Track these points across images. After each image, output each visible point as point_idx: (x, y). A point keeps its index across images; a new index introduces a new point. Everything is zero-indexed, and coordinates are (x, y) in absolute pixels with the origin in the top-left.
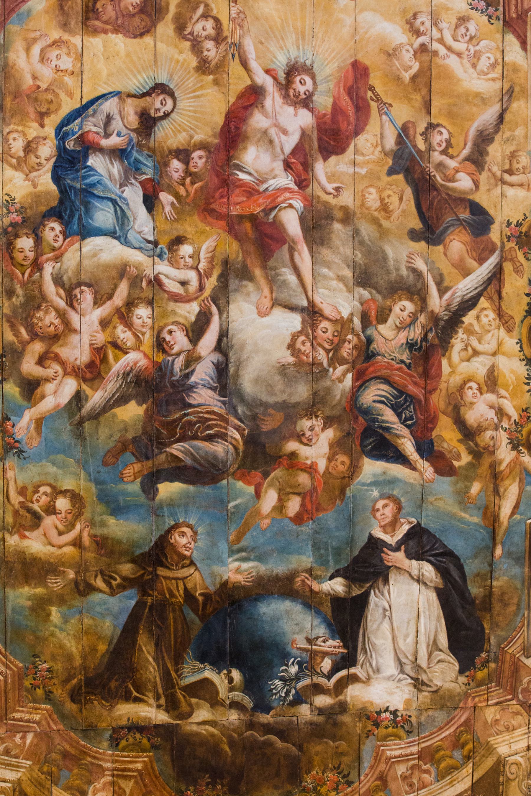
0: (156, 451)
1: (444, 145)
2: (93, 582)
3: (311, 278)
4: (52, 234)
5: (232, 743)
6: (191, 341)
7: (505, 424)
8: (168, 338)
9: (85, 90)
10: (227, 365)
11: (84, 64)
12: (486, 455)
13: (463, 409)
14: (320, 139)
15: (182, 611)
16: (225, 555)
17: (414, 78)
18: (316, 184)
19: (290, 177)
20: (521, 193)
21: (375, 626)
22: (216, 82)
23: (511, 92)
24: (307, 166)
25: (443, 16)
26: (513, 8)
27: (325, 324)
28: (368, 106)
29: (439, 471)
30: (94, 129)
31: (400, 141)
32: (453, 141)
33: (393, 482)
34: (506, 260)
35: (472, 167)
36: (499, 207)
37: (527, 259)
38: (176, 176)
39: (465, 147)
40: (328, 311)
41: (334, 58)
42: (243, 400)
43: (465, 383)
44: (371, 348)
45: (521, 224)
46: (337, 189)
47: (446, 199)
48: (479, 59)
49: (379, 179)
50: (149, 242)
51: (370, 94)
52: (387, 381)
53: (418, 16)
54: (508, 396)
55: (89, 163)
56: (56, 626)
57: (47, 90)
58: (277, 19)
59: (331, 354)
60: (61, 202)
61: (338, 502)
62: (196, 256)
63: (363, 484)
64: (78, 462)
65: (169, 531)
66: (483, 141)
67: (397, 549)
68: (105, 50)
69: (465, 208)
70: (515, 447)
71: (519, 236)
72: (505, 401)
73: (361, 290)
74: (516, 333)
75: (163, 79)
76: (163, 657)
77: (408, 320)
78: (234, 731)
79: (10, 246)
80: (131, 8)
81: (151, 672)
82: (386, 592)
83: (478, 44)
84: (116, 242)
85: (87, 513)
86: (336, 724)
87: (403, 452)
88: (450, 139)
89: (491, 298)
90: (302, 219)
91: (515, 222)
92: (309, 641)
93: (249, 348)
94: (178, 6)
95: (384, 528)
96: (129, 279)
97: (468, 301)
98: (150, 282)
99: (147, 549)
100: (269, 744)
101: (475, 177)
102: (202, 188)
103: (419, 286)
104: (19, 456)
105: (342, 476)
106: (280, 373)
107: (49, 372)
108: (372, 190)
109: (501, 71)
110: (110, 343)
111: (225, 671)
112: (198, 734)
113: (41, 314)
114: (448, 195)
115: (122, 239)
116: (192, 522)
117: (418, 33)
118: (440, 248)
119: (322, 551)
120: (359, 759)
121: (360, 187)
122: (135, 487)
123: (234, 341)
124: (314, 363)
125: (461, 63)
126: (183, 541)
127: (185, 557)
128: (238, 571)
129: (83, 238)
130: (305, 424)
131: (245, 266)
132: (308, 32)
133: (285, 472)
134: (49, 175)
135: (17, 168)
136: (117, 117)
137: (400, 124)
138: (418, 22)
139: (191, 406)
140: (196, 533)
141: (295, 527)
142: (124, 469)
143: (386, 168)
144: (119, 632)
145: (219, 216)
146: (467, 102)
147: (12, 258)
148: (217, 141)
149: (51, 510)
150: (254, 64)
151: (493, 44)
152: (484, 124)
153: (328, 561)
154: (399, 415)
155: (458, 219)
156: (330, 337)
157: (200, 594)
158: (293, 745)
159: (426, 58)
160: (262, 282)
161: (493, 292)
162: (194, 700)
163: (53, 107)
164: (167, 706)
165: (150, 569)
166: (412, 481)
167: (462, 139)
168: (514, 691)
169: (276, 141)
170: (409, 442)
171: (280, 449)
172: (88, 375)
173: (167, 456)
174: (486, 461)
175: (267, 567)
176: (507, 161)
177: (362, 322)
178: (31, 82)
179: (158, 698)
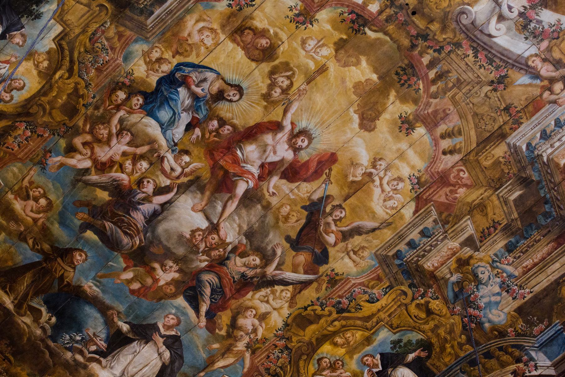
0: (99, 218)
1: (338, 218)
3: (228, 215)
4: (136, 102)
5: (29, 339)
6: (153, 192)
7: (252, 336)
8: (145, 183)
9: (206, 59)
10: (159, 214)
11: (216, 49)
12: (233, 339)
13: (240, 316)
14: (286, 169)
16: (90, 278)
17: (353, 182)
18: (267, 183)
19: (259, 171)
21: (126, 353)
22: (265, 108)
23: (390, 224)
24: (270, 174)
25: (393, 170)
26: (428, 194)
27: (215, 236)
28: (322, 175)
29: (207, 327)
30: (194, 78)
31: (321, 199)
32: (343, 220)
33: (185, 314)
36: (335, 261)
37: (326, 290)
38: (211, 127)
40: (222, 233)
41: (327, 144)
42: (153, 232)
43: (251, 308)
44: (226, 262)
45: (338, 275)
46: (274, 194)
47: (316, 238)
48: (390, 200)
49: (296, 205)
50: (174, 142)
51: (327, 171)
52: (220, 278)
53: (382, 161)
54: (264, 327)
55: (179, 89)
57: (189, 45)
58: (318, 107)
59: (207, 249)
60: (152, 93)
61: (155, 301)
62: (188, 164)
63: (172, 304)
64: (64, 193)
66: (356, 231)
67: (162, 336)
68: (231, 52)
69: (321, 248)
70: (248, 346)
71: (332, 279)
72: (261, 329)
73: (244, 238)
74: (292, 310)
75: (244, 85)
76: (30, 288)
77: (252, 266)
78: (34, 336)
79: (113, 91)
80: (259, 45)
82: (142, 346)
84: (160, 129)
85: (49, 214)
86: (76, 370)
89: (295, 289)
90: (247, 191)
92: (94, 334)
93: (175, 216)
94: (281, 63)
95: (164, 326)
96: (151, 147)
97: (285, 281)
98: (159, 156)
99: (61, 247)
100: (43, 353)
102: (217, 142)
103: (270, 258)
106: (178, 237)
107: (84, 151)
108: (288, 207)
109: (394, 213)
110: (120, 163)
112: (19, 325)
113: (102, 127)
114: (319, 237)
115: (163, 130)
116: (89, 254)
117: (374, 167)
118: (294, 253)
119: (131, 311)
121: (284, 201)
122: (78, 223)
123: (171, 209)
125: (380, 195)
126: (79, 258)
127: (74, 264)
128: (90, 287)
129: (148, 115)
130: (170, 263)
131: (205, 186)
132: (326, 124)
134: (157, 78)
135: (146, 63)
136: (209, 83)
137: (328, 193)
138: (380, 163)
139: (130, 215)
140: (86, 260)
141: (128, 293)
143: (304, 204)
144: (22, 264)
146: (366, 211)
147: (110, 95)
148: (242, 130)
149: (36, 200)
150: (289, 115)
151: (403, 200)
154: (212, 294)
155: (313, 250)
156: (213, 243)
157: (67, 281)
158: (53, 362)
159: (367, 179)
160: (206, 198)
162: (28, 312)
163: (185, 54)
165: (55, 255)
166: (193, 320)
167: (348, 222)
169: (268, 153)
171: (151, 262)
172: (99, 167)
174: (230, 341)
176: (358, 248)
177: (232, 249)
178: (186, 35)
179: (15, 299)
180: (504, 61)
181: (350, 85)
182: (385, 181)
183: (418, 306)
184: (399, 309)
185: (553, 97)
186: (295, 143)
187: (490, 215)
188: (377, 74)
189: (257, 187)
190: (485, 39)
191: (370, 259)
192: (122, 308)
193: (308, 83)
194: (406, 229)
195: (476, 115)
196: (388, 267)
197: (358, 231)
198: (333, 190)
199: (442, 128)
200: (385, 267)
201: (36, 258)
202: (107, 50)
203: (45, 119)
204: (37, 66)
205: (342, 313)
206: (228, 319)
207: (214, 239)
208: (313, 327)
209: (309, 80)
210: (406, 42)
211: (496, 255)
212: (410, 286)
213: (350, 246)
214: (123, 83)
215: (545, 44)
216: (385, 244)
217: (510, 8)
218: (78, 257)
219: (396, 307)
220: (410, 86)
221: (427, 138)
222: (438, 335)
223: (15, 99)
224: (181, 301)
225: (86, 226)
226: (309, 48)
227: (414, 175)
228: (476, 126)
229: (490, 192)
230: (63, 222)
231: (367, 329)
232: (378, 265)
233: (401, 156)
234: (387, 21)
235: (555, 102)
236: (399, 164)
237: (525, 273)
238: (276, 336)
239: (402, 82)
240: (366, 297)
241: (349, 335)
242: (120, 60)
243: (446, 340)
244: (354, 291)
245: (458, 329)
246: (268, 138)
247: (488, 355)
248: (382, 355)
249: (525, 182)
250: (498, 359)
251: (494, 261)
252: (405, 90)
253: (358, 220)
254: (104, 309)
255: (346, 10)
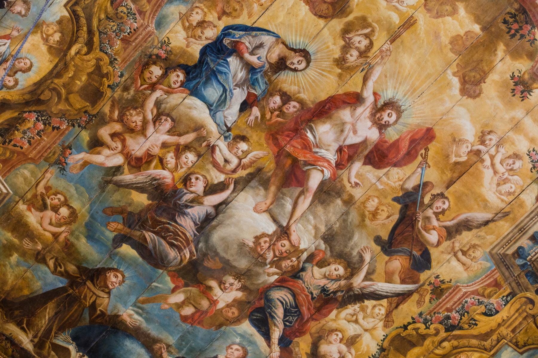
0: (137, 227)
1: (440, 210)
2: (48, 259)
3: (300, 214)
4: (176, 78)
6: (204, 192)
8: (193, 180)
9: (261, 20)
10: (213, 219)
11: (273, 6)
13: (323, 341)
14: (371, 152)
15: (83, 310)
17: (456, 163)
18: (347, 172)
19: (336, 157)
20: (459, 268)
22: (340, 76)
23: (506, 214)
24: (351, 159)
25: (507, 146)
27: (286, 242)
28: (416, 157)
30: (247, 44)
31: (417, 188)
32: (447, 213)
33: (252, 343)
34: (418, 292)
35: (444, 233)
36: (440, 265)
37: (430, 302)
38: (272, 105)
39: (450, 221)
40: (294, 237)
41: (420, 117)
42: (207, 241)
43: (336, 330)
44: (301, 273)
45: (444, 283)
46: (357, 184)
47: (413, 237)
48: (505, 183)
49: (386, 198)
50: (226, 126)
51: (423, 151)
52: (294, 295)
53: (492, 134)
54: (354, 354)
55: (228, 60)
56: (10, 263)
58: (407, 72)
59: (275, 259)
60: (195, 66)
61: (213, 328)
63: (235, 331)
64: (90, 199)
65: (110, 269)
66: (465, 226)
68: (291, 8)
69: (420, 250)
71: (437, 288)
72: (350, 356)
73: (322, 242)
74: (388, 330)
75: (311, 49)
76: (54, 322)
77: (334, 277)
79: (146, 66)
81: (42, 323)
83: (512, 176)
84: (207, 111)
85: (74, 226)
87: (271, 334)
88: (446, 210)
89: (391, 303)
90: (323, 183)
91: (442, 279)
93: (233, 220)
94: (356, 18)
96: (198, 135)
98: (208, 145)
99: (90, 268)
101: (441, 239)
102: (280, 123)
103: (357, 266)
104: (60, 171)
105: (227, 318)
106: (238, 246)
107: (113, 144)
108: (376, 200)
109: (511, 200)
110: (159, 157)
111: (81, 354)
113: (134, 113)
114: (417, 236)
115: (212, 113)
116: (126, 275)
117: (483, 142)
118: (387, 258)
119: (184, 343)
121: (370, 193)
123: (228, 211)
125: (492, 178)
126: (114, 279)
128: (130, 316)
129: (191, 94)
130: (230, 279)
132: (418, 92)
133: (198, 292)
134: (201, 47)
135: (185, 28)
136: (266, 49)
137: (425, 180)
138: (489, 137)
139: (176, 222)
141: (179, 321)
142: (113, 222)
143: (395, 195)
146: (476, 200)
147: (142, 72)
148: (312, 106)
149: (55, 209)
150: (370, 84)
151: (522, 183)
152: (474, 218)
153: (182, 350)
154: (285, 316)
155: (411, 252)
156: (283, 251)
157: (100, 310)
159: (474, 158)
160: (271, 196)
161: (395, 301)
163: (234, 14)
164: (36, 344)
166: (263, 351)
167: (453, 215)
169: (346, 133)
170: (278, 333)
171: (205, 280)
172: (133, 163)
173: (141, 234)
175: (148, 326)
176: (468, 247)
177: (307, 258)
179: (35, 337)
181: (445, 40)
182: (497, 160)
184: (525, 323)
188: (479, 23)
189: (334, 177)
191: (483, 260)
192: (172, 340)
193: (392, 41)
194: (528, 219)
196: (508, 268)
200: (504, 269)
201: (60, 283)
202: (135, 14)
203: (61, 107)
204: (46, 40)
205: (452, 331)
206: (308, 347)
207: (284, 245)
209: (393, 39)
213: (457, 246)
214: (157, 56)
216: (502, 240)
218: (112, 278)
219: (520, 319)
220: (522, 36)
223: (20, 83)
225: (120, 239)
227: (534, 150)
230: (91, 236)
231: (486, 349)
232: (494, 267)
233: (517, 126)
236: (514, 137)
239: (513, 32)
240: (482, 309)
242: (152, 27)
244: (466, 302)
246: (345, 114)
252: (516, 42)
253: (466, 211)
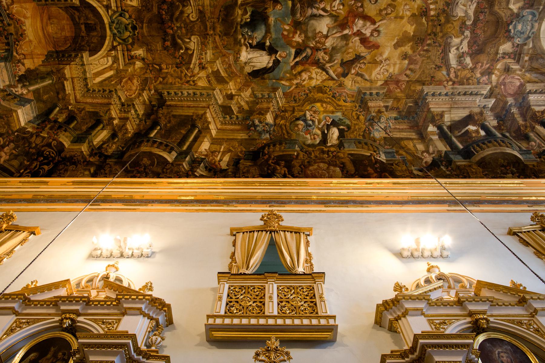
5: (233, 19)
7: (301, 82)
14: (363, 38)
17: (376, 60)
20: (350, 84)
22: (377, 14)
23: (372, 82)
24: (358, 35)
27: (324, 40)
31: (363, 56)
33: (290, 56)
35: (356, 73)
40: (327, 40)
42: (309, 21)
52: (312, 54)
65: (281, 4)
67: (275, 57)
70: (297, 84)
86: (237, 44)
90: (347, 34)
92: (256, 37)
95: (280, 54)
100: (233, 28)
112: (235, 11)
117: (385, 61)
118: (339, 66)
120: (229, 50)
124: (316, 38)
126: (279, 7)
128: (272, 20)
130: (303, 36)
131: (338, 21)
137: (366, 57)
140: (280, 10)
145: (348, 15)
150: (380, 23)
154: (304, 57)
159: (380, 63)
160: (334, 25)
162: (243, 10)
168: (244, 85)
174: (294, 77)
180: (445, 62)
181: (404, 29)
182: (384, 68)
183: (356, 114)
185: (446, 85)
186: (373, 33)
187: (399, 104)
189: (350, 36)
190: (448, 51)
192: (274, 36)
193: (395, 18)
195: (424, 71)
197: (362, 76)
198: (368, 57)
199: (412, 66)
208: (321, 95)
209: (396, 17)
210: (429, 31)
211: (390, 117)
212: (359, 106)
215: (459, 67)
217: (462, 48)
218: (279, 7)
221: (406, 66)
222: (355, 127)
224: (293, 51)
226: (406, 8)
228: (420, 75)
229: (405, 97)
233: (395, 64)
234: (431, 20)
235: (445, 87)
237: (394, 129)
238: (308, 88)
240: (344, 99)
241: (329, 106)
243: (356, 130)
245: (363, 130)
246: (368, 24)
247: (366, 144)
248: (333, 120)
249: (416, 103)
250: (368, 147)
251: (388, 118)
254: (268, 31)
255: (425, 6)
